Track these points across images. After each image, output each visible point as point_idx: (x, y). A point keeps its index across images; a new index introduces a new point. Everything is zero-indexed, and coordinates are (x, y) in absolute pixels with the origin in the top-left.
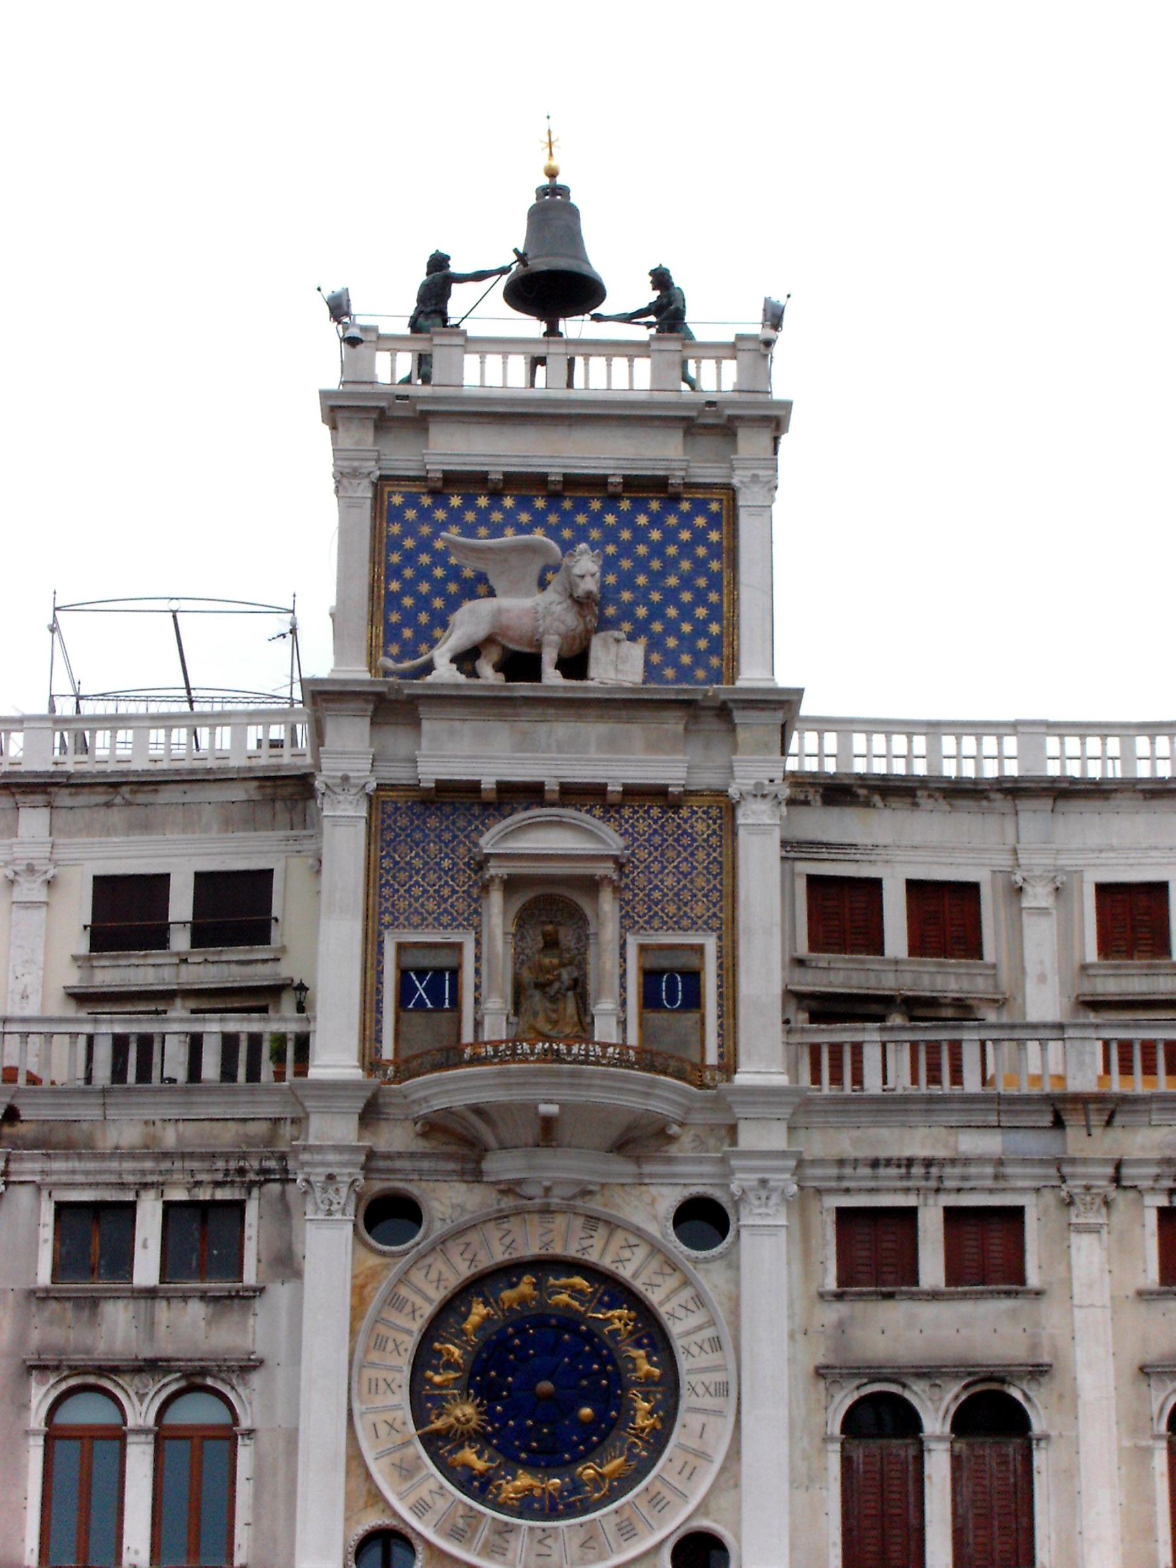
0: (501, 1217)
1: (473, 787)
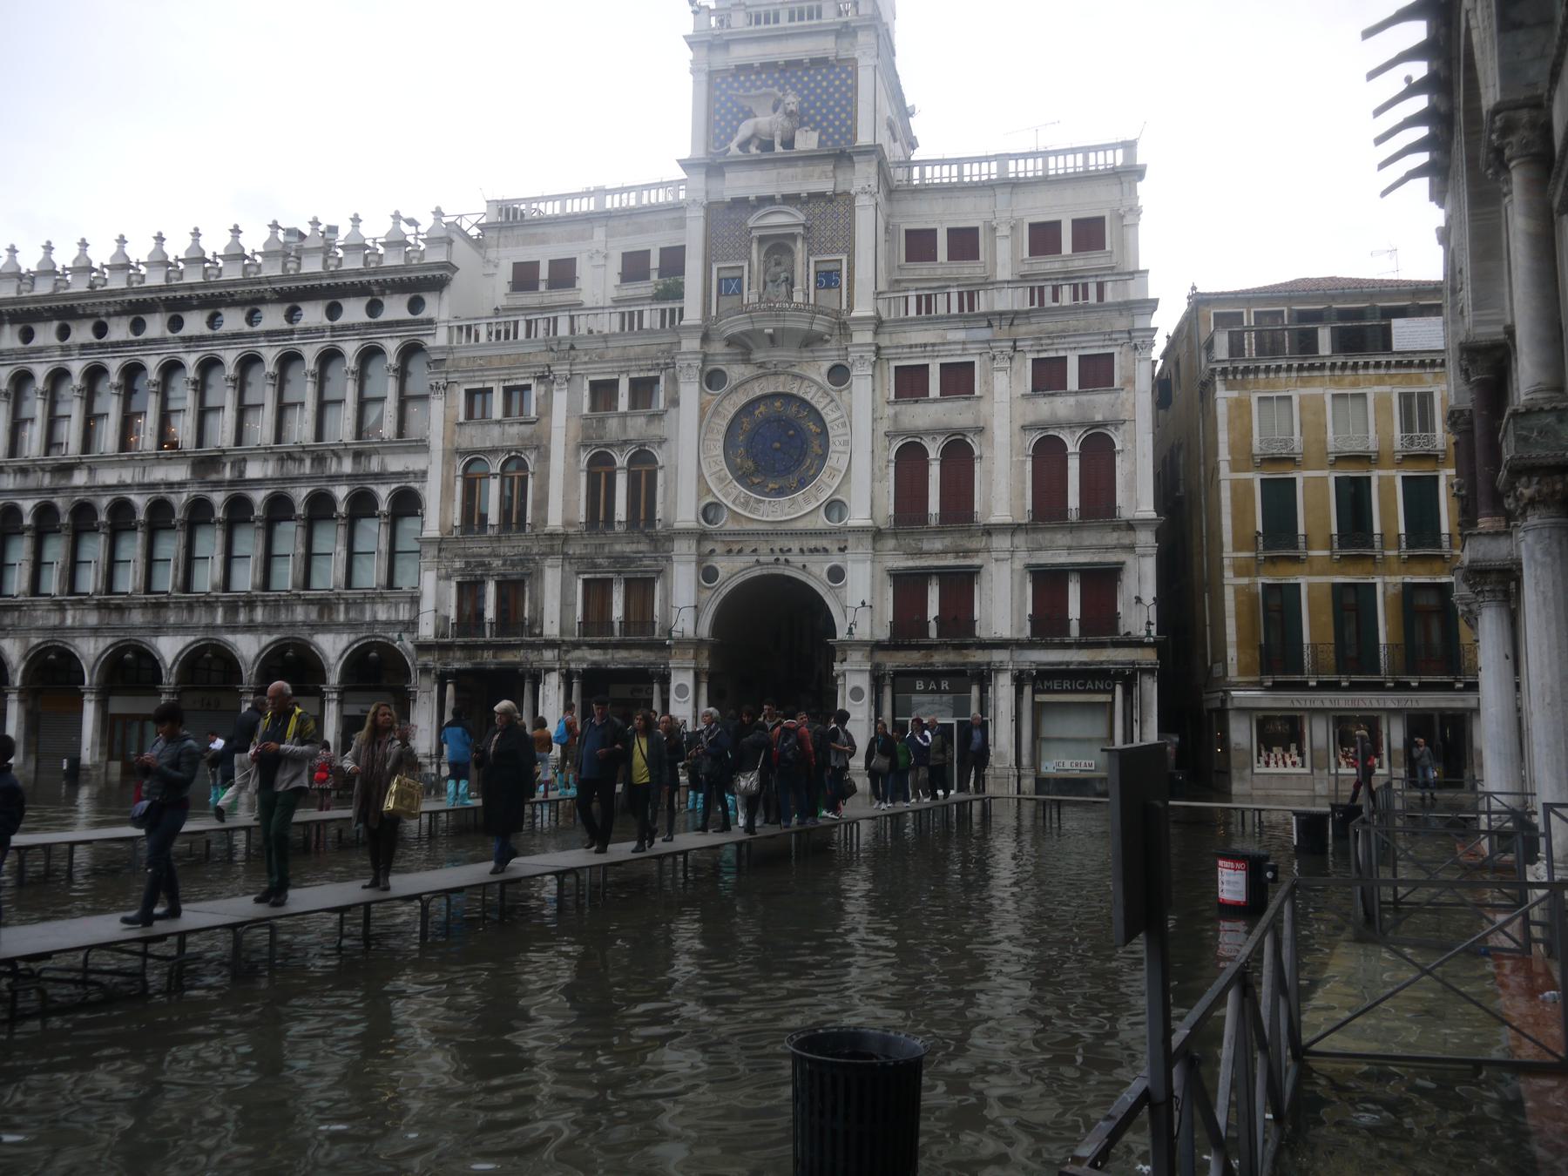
0: (758, 377)
1: (746, 200)
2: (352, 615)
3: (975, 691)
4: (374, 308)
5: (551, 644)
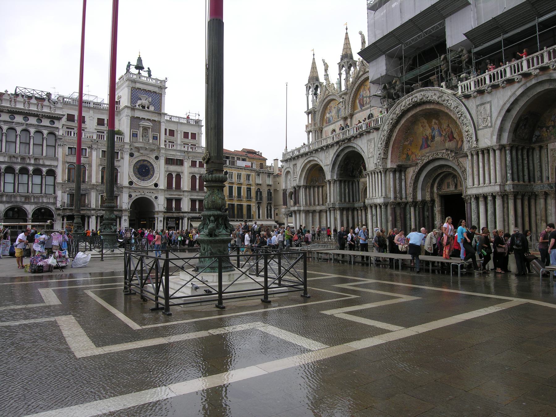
2: (36, 200)
3: (181, 221)
4: (40, 120)
5: (94, 210)
